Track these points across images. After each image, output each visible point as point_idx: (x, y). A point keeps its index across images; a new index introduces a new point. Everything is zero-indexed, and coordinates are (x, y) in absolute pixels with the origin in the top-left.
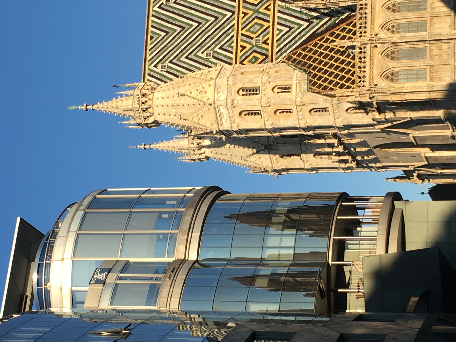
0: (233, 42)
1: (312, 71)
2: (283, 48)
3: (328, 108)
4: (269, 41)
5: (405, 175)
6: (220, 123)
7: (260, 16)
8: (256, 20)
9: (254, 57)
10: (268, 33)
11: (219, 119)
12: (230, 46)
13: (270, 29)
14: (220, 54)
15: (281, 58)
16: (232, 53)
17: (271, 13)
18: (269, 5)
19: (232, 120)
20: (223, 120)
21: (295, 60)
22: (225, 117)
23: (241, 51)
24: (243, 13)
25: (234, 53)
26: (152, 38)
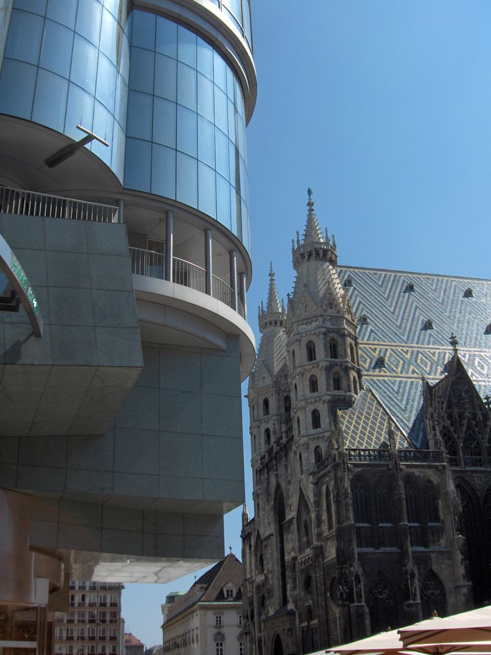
0: (379, 341)
1: (357, 411)
2: (378, 385)
3: (320, 427)
4: (382, 373)
5: (249, 521)
6: (301, 323)
7: (406, 366)
8: (402, 362)
9: (366, 359)
10: (390, 372)
11: (305, 322)
12: (375, 339)
13: (395, 374)
14: (366, 330)
15: (367, 383)
16: (368, 340)
17: (410, 375)
18: (418, 374)
19: (304, 335)
20: (304, 326)
21: (367, 396)
22: (307, 327)
23: (370, 348)
24: (407, 351)
25: (369, 342)
26: (376, 274)
